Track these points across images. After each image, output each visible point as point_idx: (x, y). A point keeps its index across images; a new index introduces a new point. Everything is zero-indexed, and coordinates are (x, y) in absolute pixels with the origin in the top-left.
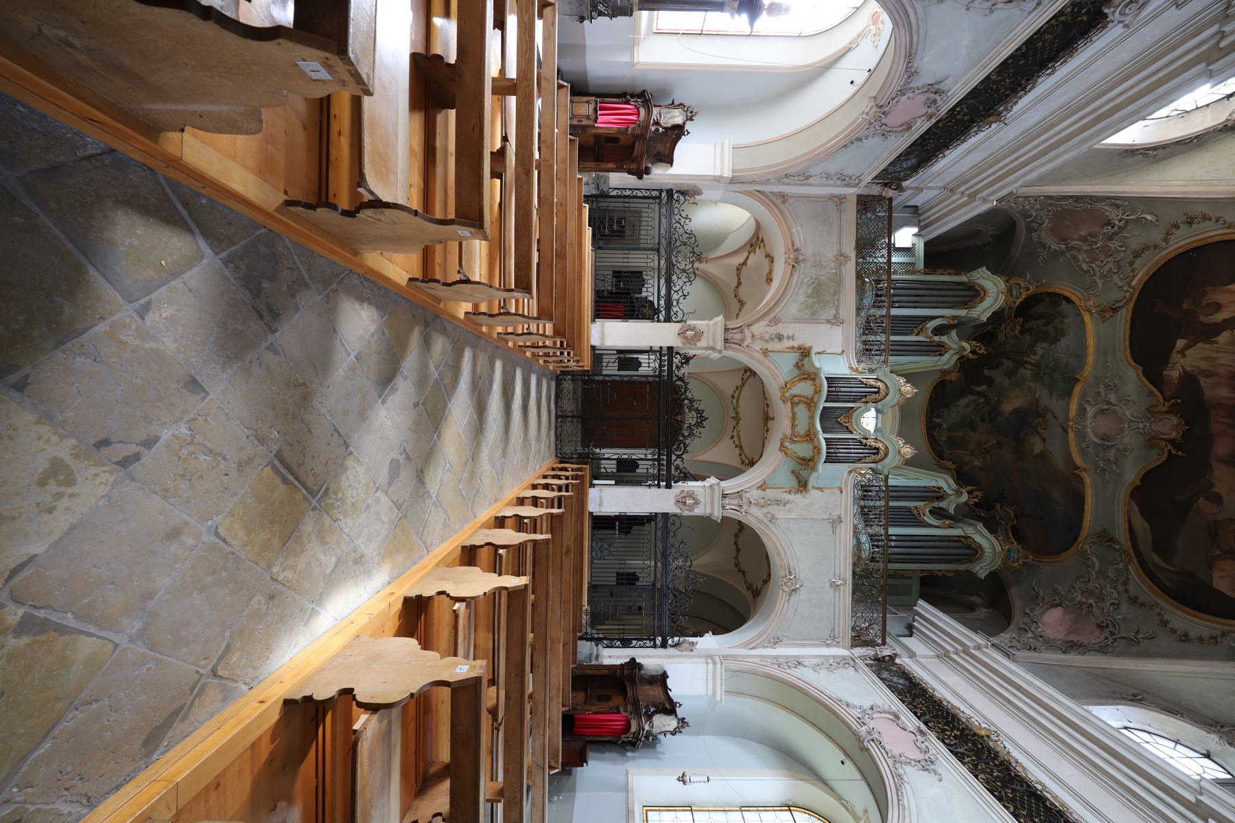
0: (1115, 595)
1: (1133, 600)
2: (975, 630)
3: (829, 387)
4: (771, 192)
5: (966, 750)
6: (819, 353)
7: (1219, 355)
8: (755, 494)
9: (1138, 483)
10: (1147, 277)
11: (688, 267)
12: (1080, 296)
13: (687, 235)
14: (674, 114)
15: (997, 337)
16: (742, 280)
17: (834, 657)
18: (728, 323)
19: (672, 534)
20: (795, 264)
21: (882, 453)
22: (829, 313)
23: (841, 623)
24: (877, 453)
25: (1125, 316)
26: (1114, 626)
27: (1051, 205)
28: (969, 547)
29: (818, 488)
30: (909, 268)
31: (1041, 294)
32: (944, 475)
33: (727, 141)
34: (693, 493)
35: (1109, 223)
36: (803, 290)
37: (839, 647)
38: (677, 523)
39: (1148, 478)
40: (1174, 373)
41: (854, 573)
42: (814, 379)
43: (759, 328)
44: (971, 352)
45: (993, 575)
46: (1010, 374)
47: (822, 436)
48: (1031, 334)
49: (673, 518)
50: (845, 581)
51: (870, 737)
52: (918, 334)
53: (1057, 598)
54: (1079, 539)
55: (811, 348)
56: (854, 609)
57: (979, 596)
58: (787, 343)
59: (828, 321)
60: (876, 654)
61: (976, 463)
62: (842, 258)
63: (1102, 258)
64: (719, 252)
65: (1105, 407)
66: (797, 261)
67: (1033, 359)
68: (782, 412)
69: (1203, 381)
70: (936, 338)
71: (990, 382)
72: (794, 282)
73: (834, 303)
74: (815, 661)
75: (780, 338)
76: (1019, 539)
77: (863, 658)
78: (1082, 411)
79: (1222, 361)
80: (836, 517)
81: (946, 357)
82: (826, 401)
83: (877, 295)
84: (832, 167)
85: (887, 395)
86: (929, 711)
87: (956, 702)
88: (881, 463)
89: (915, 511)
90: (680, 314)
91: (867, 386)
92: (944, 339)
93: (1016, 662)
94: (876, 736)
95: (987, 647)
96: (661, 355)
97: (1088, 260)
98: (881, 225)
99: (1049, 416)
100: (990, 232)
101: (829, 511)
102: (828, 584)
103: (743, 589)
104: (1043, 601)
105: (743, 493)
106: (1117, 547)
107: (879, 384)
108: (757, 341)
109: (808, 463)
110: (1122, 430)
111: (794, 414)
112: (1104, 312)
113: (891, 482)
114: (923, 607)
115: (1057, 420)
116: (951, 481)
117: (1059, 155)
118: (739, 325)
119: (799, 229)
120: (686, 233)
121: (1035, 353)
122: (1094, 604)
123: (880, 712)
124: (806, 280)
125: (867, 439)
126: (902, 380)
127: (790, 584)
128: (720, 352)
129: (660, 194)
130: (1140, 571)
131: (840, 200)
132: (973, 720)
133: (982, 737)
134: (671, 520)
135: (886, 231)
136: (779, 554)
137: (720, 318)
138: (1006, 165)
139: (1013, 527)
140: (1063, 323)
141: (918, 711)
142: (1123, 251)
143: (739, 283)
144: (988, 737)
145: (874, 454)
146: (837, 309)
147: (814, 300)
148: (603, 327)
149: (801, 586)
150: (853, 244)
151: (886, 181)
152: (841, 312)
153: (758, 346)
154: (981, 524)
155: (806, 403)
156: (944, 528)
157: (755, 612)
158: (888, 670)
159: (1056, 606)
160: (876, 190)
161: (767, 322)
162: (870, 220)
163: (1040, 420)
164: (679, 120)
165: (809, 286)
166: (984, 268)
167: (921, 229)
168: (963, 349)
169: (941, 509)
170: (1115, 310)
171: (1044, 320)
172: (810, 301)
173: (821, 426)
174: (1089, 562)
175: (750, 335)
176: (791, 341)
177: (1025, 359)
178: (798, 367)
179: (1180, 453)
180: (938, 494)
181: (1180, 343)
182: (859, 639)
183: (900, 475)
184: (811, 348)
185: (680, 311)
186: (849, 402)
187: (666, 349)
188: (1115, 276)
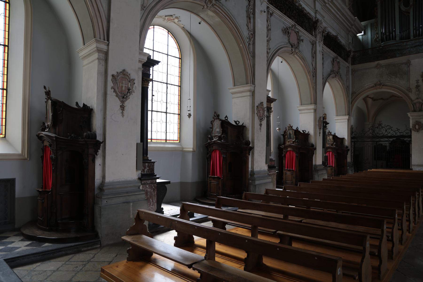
4: (351, 98)
11: (384, 129)
13: (370, 130)
14: (329, 139)
20: (382, 85)
30: (373, 27)
33: (335, 118)
43: (413, 96)
59: (409, 67)
64: (365, 110)
66: (380, 84)
72: (390, 84)
75: (418, 87)
90: (407, 131)
118: (412, 105)
119: (367, 85)
120: (369, 131)
129: (353, 142)
131: (354, 71)
138: (346, 23)
143: (382, 99)
148: (415, 165)
160: (350, 59)
161: (410, 93)
164: (331, 137)
185: (405, 132)
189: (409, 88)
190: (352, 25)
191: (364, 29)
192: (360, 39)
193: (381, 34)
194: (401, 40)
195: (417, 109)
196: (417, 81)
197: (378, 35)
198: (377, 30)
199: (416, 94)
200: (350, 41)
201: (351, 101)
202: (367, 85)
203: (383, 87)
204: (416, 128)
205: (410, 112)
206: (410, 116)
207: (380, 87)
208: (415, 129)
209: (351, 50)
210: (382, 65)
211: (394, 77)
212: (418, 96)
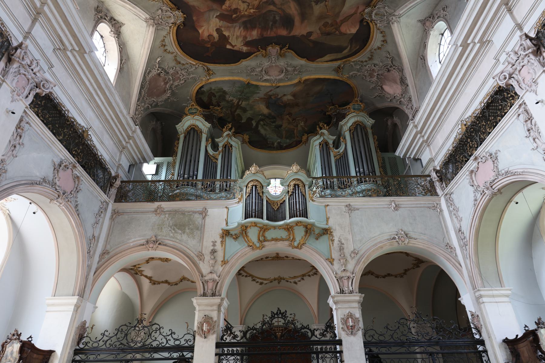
0: (370, 65)
1: (370, 59)
2: (406, 126)
3: (252, 217)
5: (477, 136)
6: (227, 223)
7: (235, 34)
8: (337, 266)
9: (305, 59)
10: (191, 59)
12: (199, 83)
15: (221, 117)
16: (164, 280)
17: (448, 207)
18: (199, 293)
19: (382, 338)
20: (158, 243)
21: (298, 182)
22: (198, 218)
23: (422, 203)
24: (298, 185)
25: (211, 66)
26: (387, 66)
27: (143, 98)
28: (356, 128)
29: (327, 221)
31: (196, 99)
32: (311, 142)
34: (343, 319)
35: (159, 75)
36: (179, 237)
37: (440, 204)
38: (372, 332)
39: (301, 55)
40: (245, 49)
41: (385, 196)
42: (246, 227)
43: (205, 268)
44: (230, 131)
45: (371, 115)
46: (245, 110)
47: (288, 221)
48: (220, 102)
49: (367, 336)
50: (391, 201)
51: (490, 188)
53: (378, 88)
54: (341, 79)
55: (223, 229)
56: (410, 194)
57: (387, 121)
58: (218, 247)
59: (204, 218)
60: (437, 180)
61: (302, 124)
62: (158, 211)
63: (178, 75)
64: (137, 301)
65: (264, 72)
66: (155, 242)
67: (235, 101)
68: (270, 248)
69: (249, 39)
70: (220, 149)
71: (250, 119)
72: (171, 243)
73: (191, 215)
74: (455, 220)
75: (214, 252)
76: (347, 103)
77: (443, 189)
78: (266, 81)
79: (239, 34)
80: (347, 208)
81: (232, 143)
82: (262, 218)
83: (188, 185)
84: (90, 218)
85: (257, 181)
86: (462, 154)
87: (452, 140)
88: (305, 183)
89: (337, 157)
92: (221, 145)
93: (420, 107)
94: (488, 185)
95: (414, 122)
96: (223, 354)
97: (179, 81)
98: (139, 187)
99: (270, 93)
100: (154, 123)
101: (343, 213)
102: (396, 212)
103: (419, 271)
104: (381, 94)
105: (338, 276)
106: (342, 65)
107: (250, 185)
108: (216, 268)
109: (309, 229)
110: (276, 66)
111: (273, 240)
112: (210, 74)
113: (319, 175)
114: (400, 152)
115: (272, 90)
116: (315, 138)
117: (116, 101)
118: (201, 284)
119: (131, 241)
121: (233, 100)
122: (377, 73)
123: (473, 181)
124: (171, 235)
125: (288, 191)
126: (248, 172)
128: (222, 299)
130: (354, 57)
131: (115, 213)
132: (459, 132)
133: (466, 128)
134: (370, 339)
135: (144, 184)
136: (382, 247)
137: (195, 301)
139: (340, 106)
140: (214, 90)
141: (464, 159)
142: (176, 68)
144: (465, 125)
145: (298, 187)
146: (195, 212)
147: (187, 228)
150: (149, 203)
151: (109, 186)
152: (198, 210)
153: (219, 268)
154: (340, 123)
155: (264, 231)
156: (346, 141)
157: (432, 262)
158: (446, 174)
159: (382, 87)
160: (113, 191)
161: (201, 262)
162: (133, 194)
163: (272, 97)
165: (176, 232)
166: (176, 126)
167: (146, 161)
168: (228, 135)
169: (334, 143)
170: (209, 70)
171: (212, 97)
172: (187, 231)
173: (280, 221)
174: (354, 75)
175: (210, 275)
176: (216, 244)
177: (235, 104)
178: (237, 238)
179: (287, 46)
180: (324, 146)
181: (228, 47)
182: (431, 191)
183: (314, 166)
184: (223, 229)
186: (262, 203)
187: (218, 350)
188: (189, 70)
189: (201, 254)
190: (129, 137)
195: (209, 291)
202: (133, 240)
203: (160, 246)
204: (202, 330)
205: (198, 297)
206: (196, 305)
207: (155, 246)
208: (201, 332)
211: (180, 232)
212: (212, 268)
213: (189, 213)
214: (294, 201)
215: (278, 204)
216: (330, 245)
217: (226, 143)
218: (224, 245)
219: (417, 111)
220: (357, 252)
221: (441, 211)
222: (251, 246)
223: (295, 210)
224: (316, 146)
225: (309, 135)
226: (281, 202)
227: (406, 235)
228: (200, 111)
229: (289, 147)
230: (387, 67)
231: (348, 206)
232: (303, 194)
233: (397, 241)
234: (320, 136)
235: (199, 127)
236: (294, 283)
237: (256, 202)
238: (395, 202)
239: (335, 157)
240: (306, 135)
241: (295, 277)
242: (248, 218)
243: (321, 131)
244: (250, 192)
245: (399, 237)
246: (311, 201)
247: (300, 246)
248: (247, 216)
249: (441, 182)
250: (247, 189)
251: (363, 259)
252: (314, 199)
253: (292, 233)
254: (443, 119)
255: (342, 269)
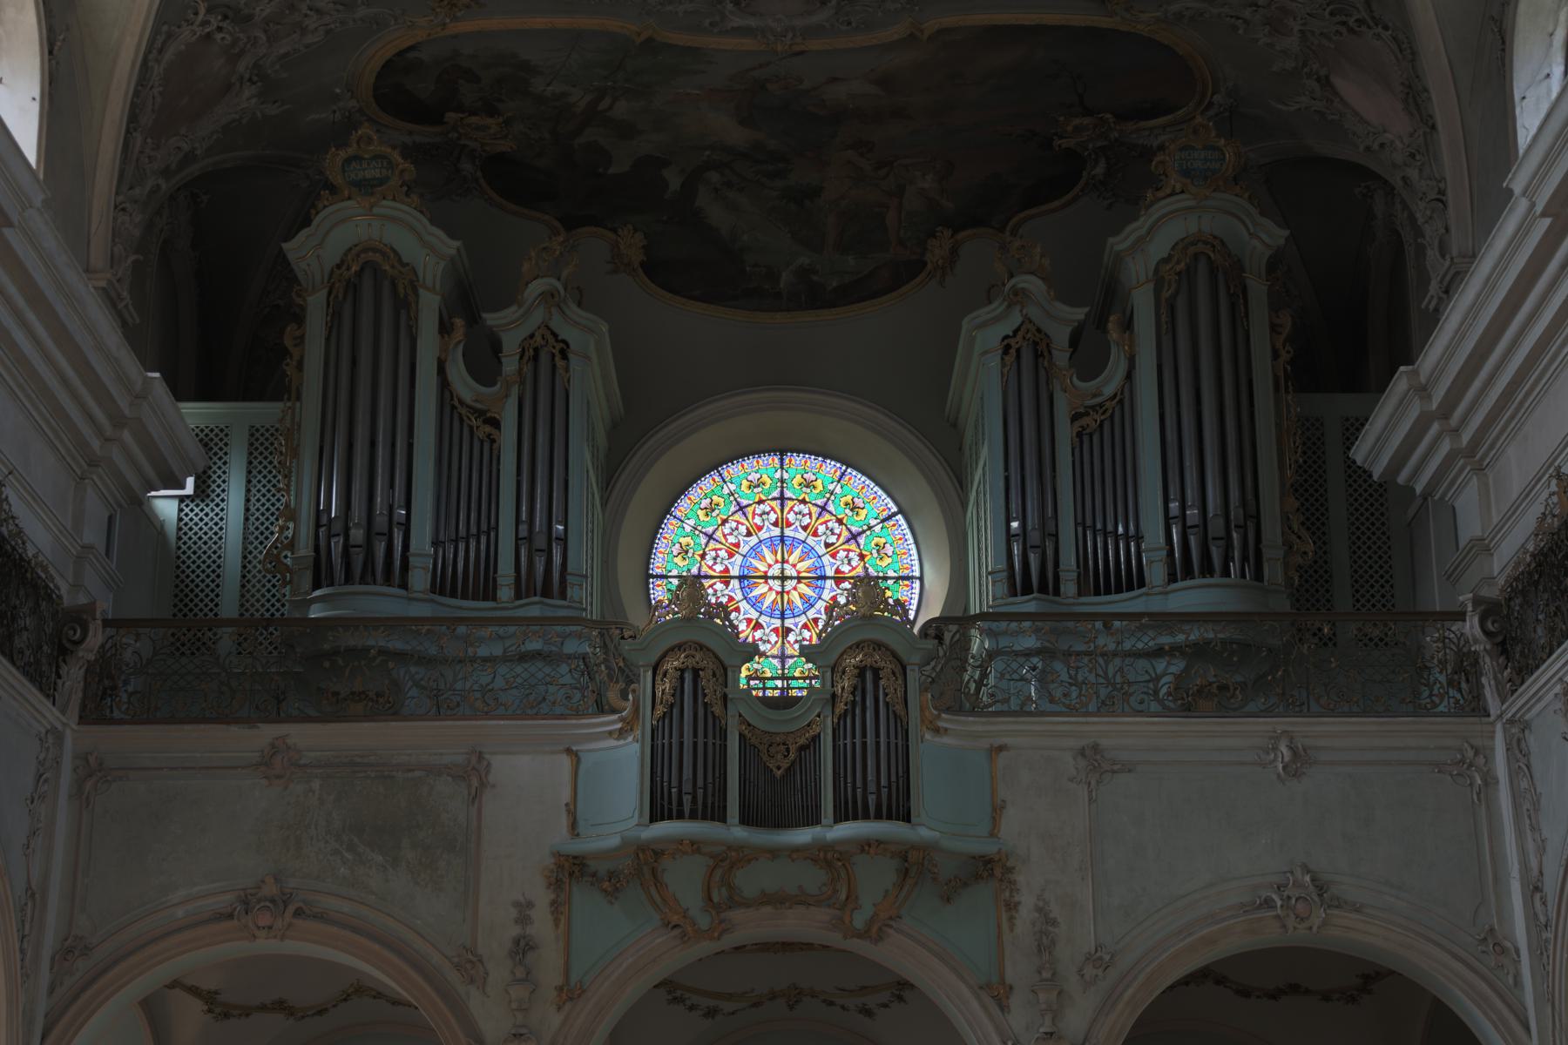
3: (680, 816)
4: (51, 990)
8: (1019, 1017)
17: (1513, 776)
20: (291, 909)
24: (876, 672)
32: (966, 324)
52: (495, 423)
55: (557, 855)
59: (475, 798)
70: (510, 365)
75: (523, 948)
82: (723, 819)
85: (701, 647)
89: (1084, 421)
91: (674, 708)
92: (511, 343)
95: (1416, 373)
107: (672, 664)
111: (766, 899)
116: (983, 313)
127: (1300, 906)
143: (280, 1006)
145: (876, 678)
149: (1306, 869)
154: (1111, 240)
160: (73, 676)
166: (285, 246)
168: (549, 296)
169: (1074, 341)
184: (557, 855)
186: (724, 748)
189: (470, 957)
190: (119, 421)
191: (201, 470)
192: (162, 524)
193: (318, 525)
194: (442, 593)
196: (523, 911)
197: (291, 525)
198: (288, 486)
199: (510, 1002)
200: (93, 535)
201: (46, 1016)
209: (91, 608)
210: (302, 762)
213: (410, 775)
214: (858, 741)
215: (788, 750)
216: (999, 926)
217: (538, 338)
218: (563, 919)
219: (1457, 273)
220: (1107, 958)
221: (1486, 783)
222: (676, 926)
223: (859, 784)
224: (985, 353)
225: (961, 235)
226: (802, 741)
227: (1321, 887)
228: (402, 171)
229: (855, 292)
230: (1344, 18)
231: (1091, 754)
232: (894, 711)
233: (1278, 917)
234: (1009, 306)
235: (400, 260)
236: (860, 1012)
237: (695, 744)
238: (1291, 739)
239: (1077, 424)
240: (947, 233)
241: (863, 988)
242: (662, 819)
243: (1013, 281)
244: (671, 700)
245: (1289, 898)
246: (928, 736)
247: (874, 929)
248: (659, 809)
249: (1501, 660)
250: (658, 678)
251: (1130, 991)
252: (941, 724)
253: (843, 875)
254: (1521, 403)
255: (1042, 1030)
